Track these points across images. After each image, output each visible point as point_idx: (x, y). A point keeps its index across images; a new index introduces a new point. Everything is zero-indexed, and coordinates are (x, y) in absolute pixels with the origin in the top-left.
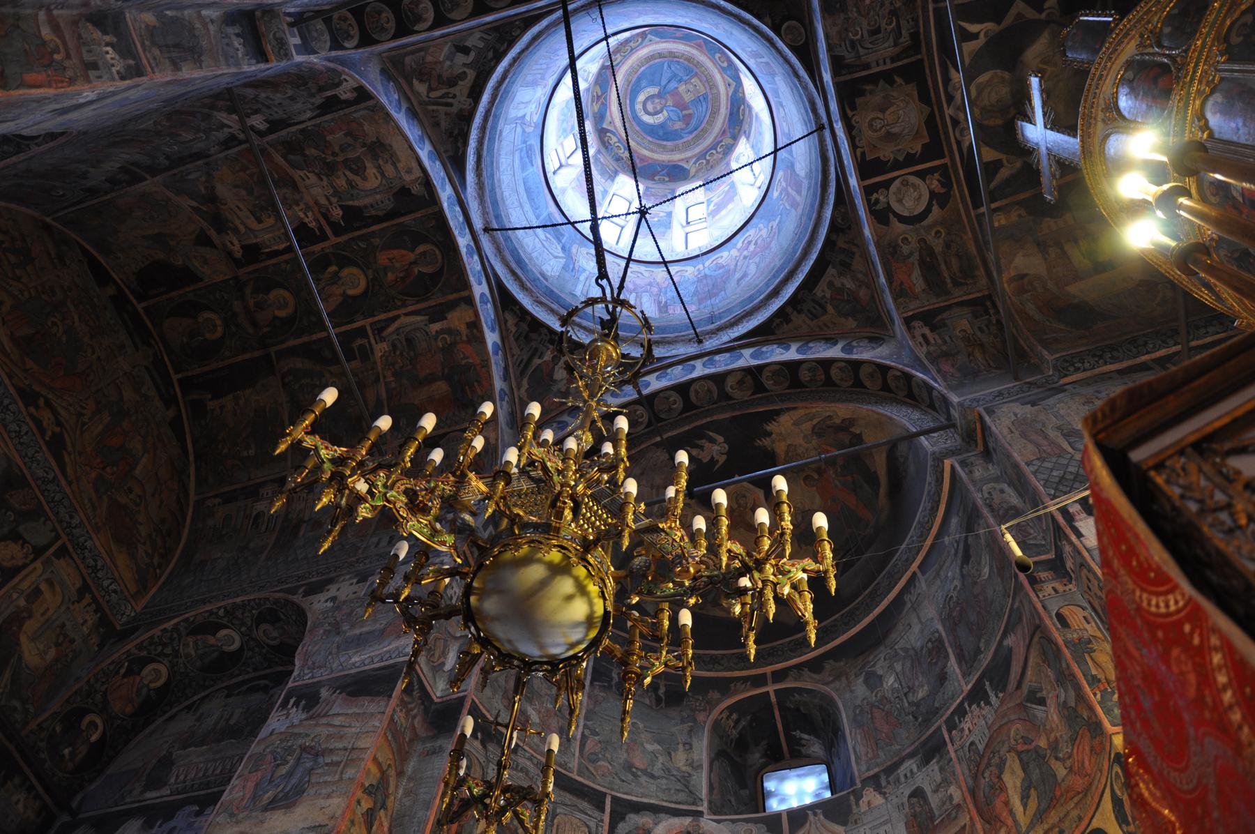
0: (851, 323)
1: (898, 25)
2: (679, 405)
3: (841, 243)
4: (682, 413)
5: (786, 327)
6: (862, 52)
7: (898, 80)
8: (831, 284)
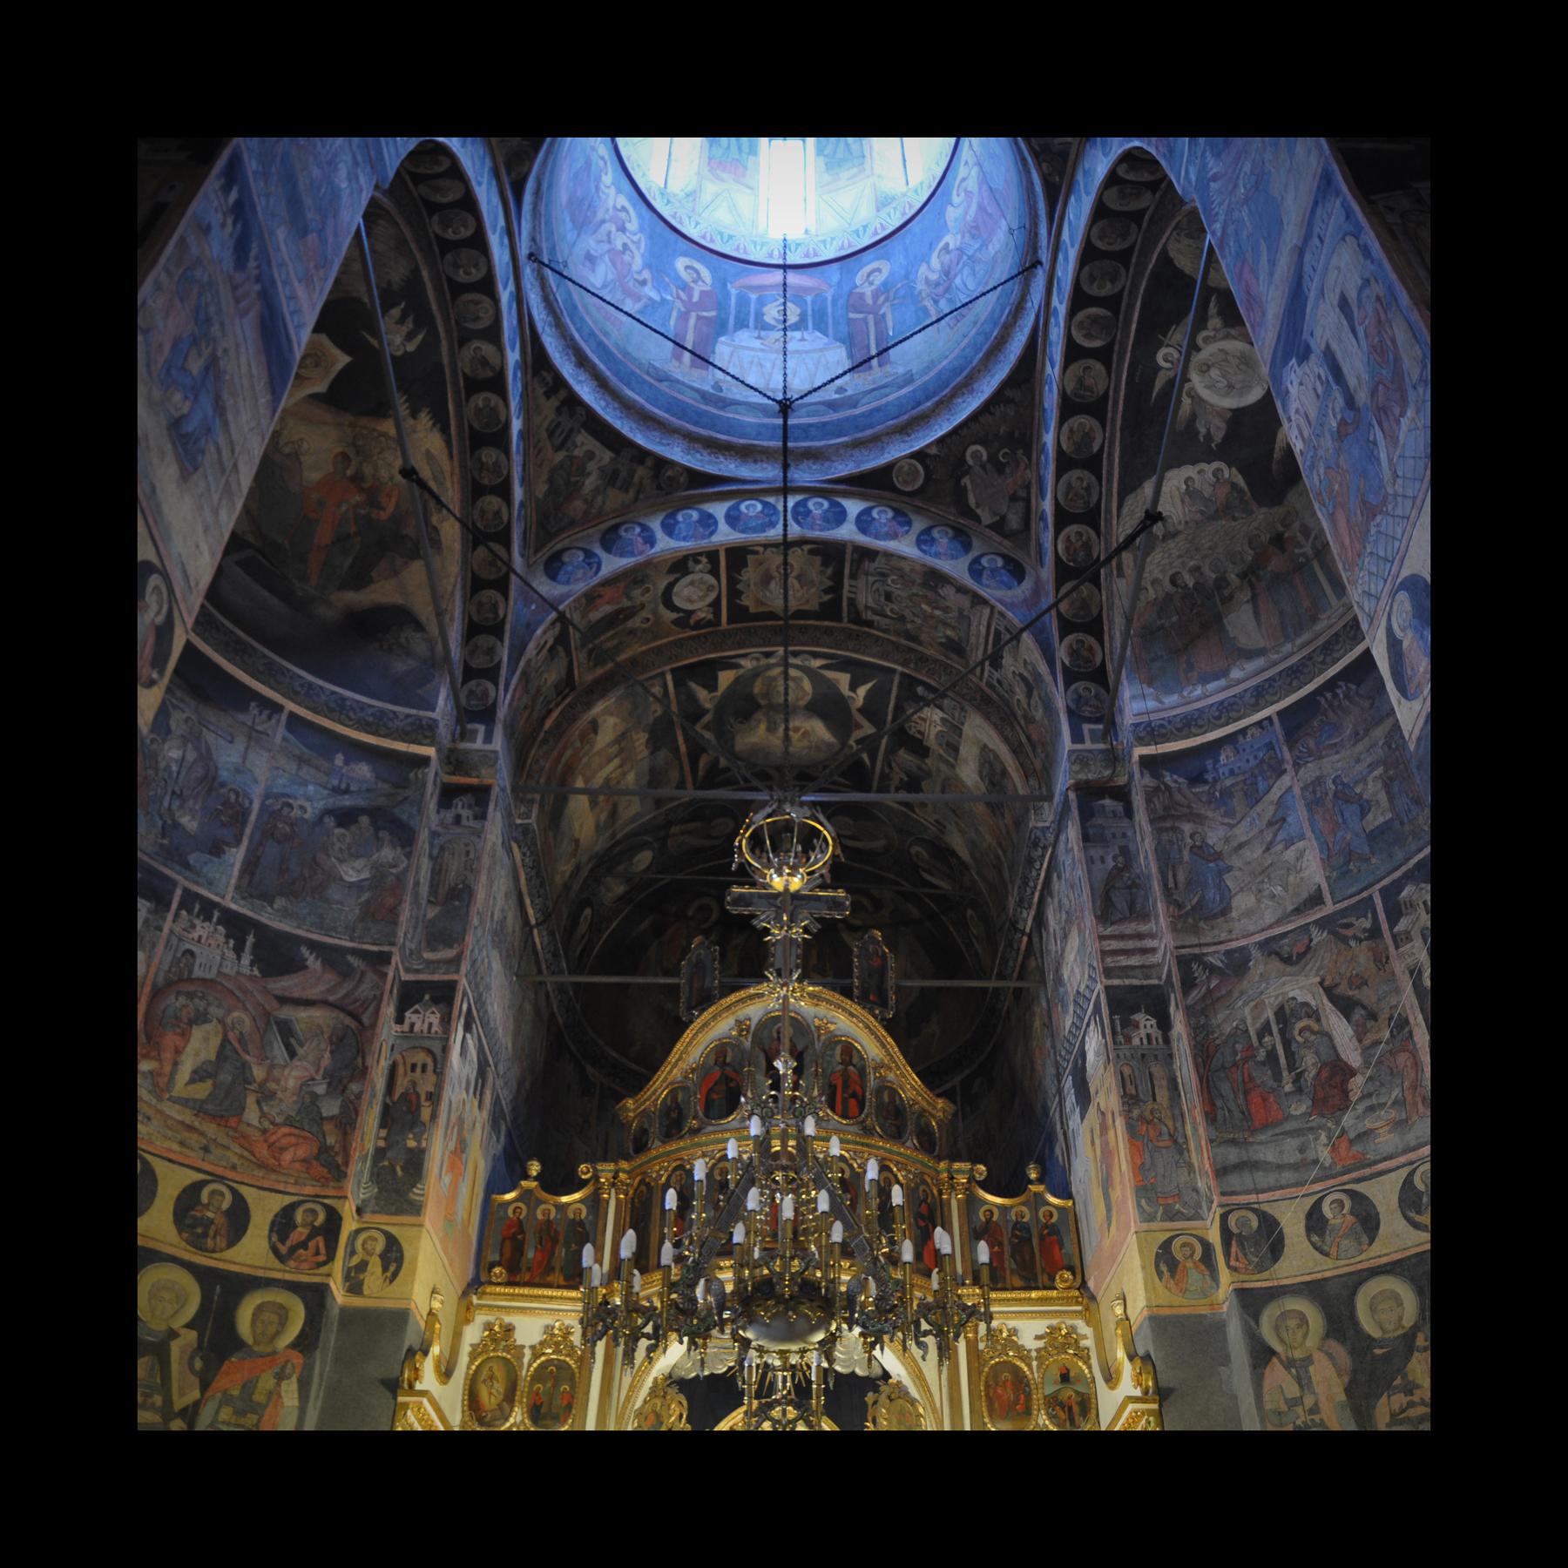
0: (541, 489)
1: (886, 616)
2: (461, 277)
3: (641, 472)
4: (450, 280)
5: (540, 391)
6: (871, 579)
7: (827, 598)
8: (590, 455)
